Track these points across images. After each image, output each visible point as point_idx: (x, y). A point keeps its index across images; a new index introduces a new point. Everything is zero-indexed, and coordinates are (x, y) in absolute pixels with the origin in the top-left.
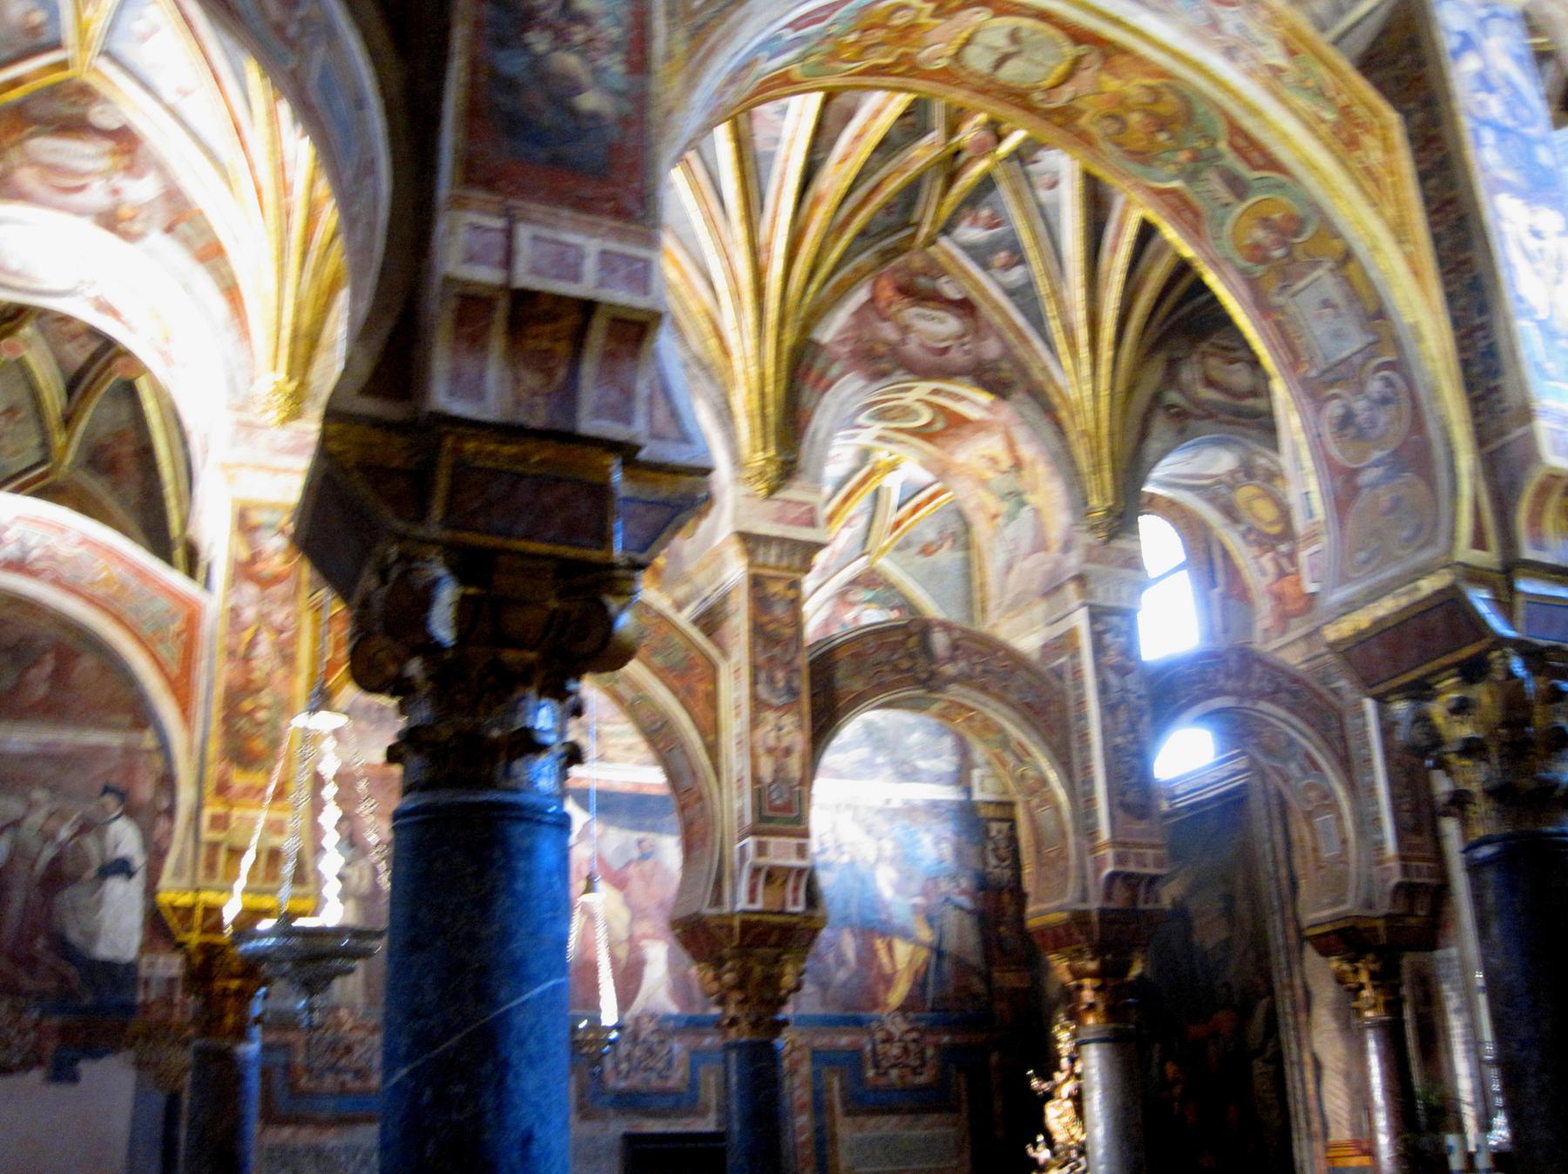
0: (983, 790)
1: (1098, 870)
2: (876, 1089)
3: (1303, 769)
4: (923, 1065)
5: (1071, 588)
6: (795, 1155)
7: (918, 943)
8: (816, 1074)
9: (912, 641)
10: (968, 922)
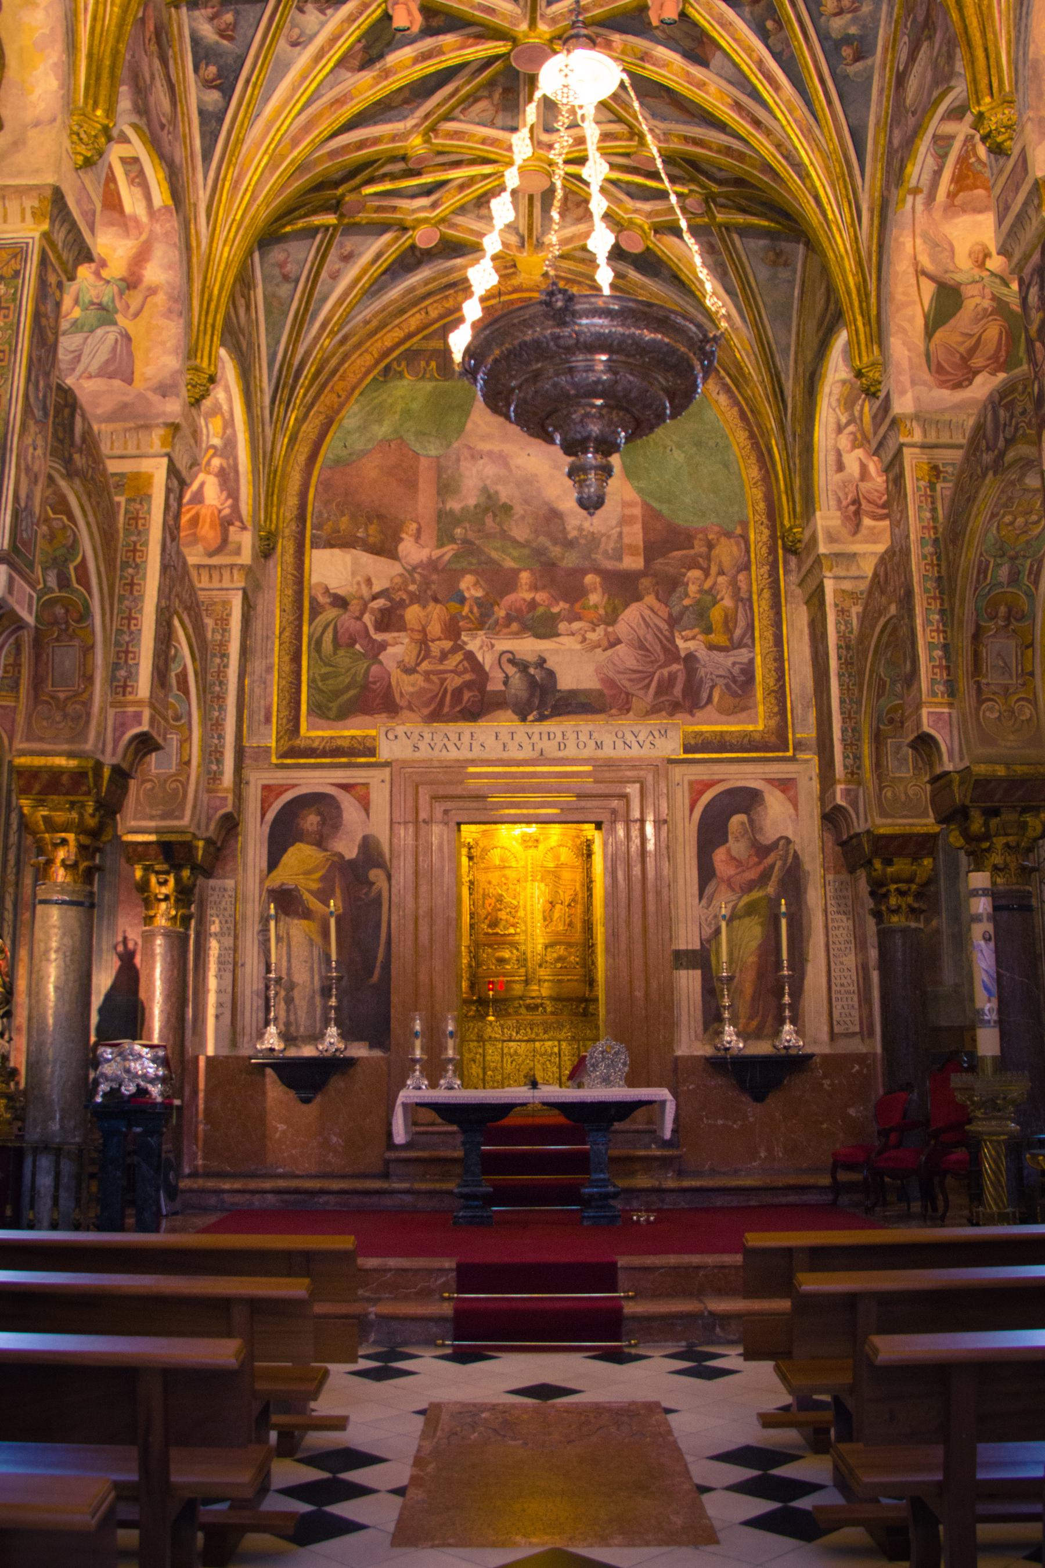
1: (121, 727)
9: (67, 411)
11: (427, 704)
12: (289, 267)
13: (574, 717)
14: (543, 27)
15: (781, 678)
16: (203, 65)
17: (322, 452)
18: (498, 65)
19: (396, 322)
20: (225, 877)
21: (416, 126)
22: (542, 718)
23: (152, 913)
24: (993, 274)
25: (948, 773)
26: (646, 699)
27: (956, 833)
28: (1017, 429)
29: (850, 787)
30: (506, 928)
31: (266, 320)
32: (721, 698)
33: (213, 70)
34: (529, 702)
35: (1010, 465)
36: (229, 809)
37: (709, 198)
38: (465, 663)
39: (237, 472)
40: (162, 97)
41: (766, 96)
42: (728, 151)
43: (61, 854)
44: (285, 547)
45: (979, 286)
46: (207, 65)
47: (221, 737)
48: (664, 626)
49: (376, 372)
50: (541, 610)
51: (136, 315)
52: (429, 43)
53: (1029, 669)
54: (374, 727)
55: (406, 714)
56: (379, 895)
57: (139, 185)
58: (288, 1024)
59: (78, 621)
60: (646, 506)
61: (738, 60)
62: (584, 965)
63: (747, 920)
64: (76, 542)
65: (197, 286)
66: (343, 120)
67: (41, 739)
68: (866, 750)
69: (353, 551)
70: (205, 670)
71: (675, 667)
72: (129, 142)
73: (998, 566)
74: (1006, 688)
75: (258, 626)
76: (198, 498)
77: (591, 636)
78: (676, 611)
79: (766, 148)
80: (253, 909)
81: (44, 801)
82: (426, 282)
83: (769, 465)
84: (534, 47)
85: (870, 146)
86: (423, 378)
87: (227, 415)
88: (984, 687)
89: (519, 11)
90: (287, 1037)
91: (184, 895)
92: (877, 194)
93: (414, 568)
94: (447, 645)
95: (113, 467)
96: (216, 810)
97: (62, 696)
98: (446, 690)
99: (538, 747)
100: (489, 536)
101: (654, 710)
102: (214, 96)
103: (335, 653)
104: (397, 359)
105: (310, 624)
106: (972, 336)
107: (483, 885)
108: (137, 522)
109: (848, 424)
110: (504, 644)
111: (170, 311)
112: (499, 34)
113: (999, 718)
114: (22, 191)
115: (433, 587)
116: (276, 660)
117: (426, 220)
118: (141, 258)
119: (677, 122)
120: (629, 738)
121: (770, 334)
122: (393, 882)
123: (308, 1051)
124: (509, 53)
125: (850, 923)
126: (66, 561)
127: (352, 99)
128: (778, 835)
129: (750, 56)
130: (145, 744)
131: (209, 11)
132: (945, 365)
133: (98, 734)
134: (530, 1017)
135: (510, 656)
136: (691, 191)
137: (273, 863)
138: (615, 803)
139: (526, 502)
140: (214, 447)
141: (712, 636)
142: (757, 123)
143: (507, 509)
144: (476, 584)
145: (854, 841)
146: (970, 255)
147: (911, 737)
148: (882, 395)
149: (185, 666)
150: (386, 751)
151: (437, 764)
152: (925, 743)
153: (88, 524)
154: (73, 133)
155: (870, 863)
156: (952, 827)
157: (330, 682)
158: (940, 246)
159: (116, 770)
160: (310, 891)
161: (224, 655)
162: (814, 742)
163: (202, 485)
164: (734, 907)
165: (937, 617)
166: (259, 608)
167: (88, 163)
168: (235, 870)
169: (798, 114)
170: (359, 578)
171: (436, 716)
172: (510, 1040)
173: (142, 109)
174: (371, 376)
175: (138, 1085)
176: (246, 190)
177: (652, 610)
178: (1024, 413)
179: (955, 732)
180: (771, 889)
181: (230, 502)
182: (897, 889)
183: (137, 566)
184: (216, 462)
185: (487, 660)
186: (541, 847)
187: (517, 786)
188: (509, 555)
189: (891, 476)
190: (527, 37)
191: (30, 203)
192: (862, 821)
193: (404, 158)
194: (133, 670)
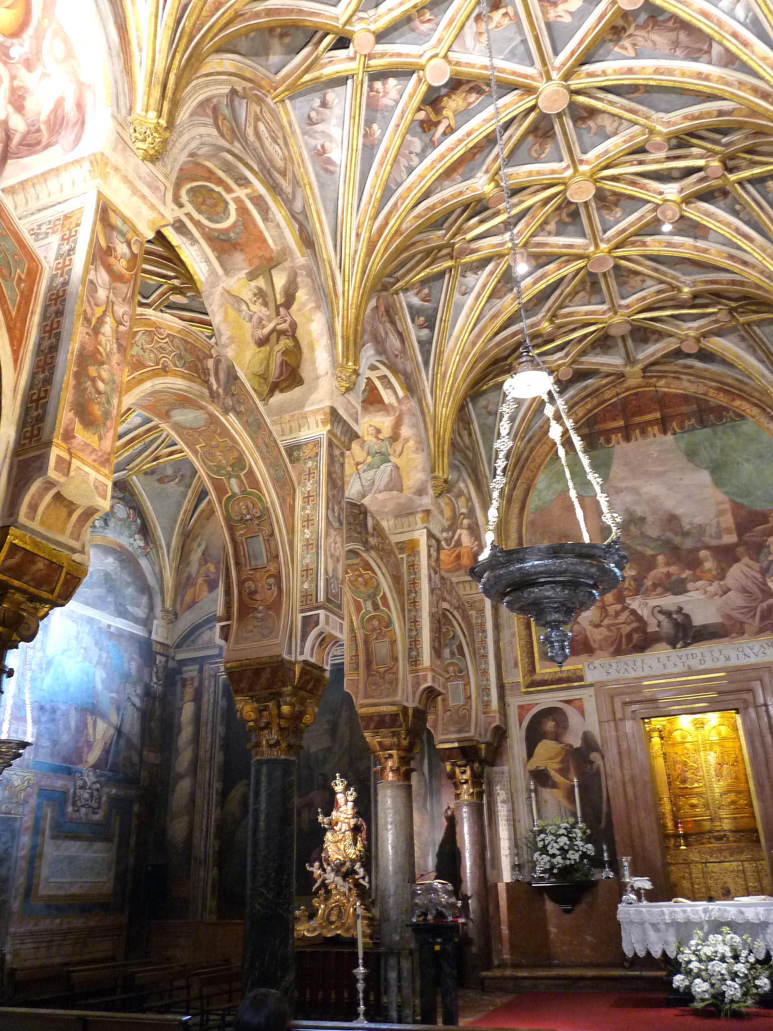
0: (157, 634)
1: (417, 684)
2: (71, 820)
3: (452, 654)
4: (99, 808)
5: (419, 517)
6: (15, 867)
7: (109, 723)
8: (39, 806)
9: (361, 516)
10: (136, 715)
11: (612, 644)
12: (490, 408)
13: (706, 642)
14: (603, 246)
16: (416, 318)
18: (583, 272)
22: (686, 645)
33: (422, 319)
34: (676, 636)
37: (731, 311)
38: (631, 617)
39: (477, 525)
40: (394, 340)
41: (745, 247)
42: (733, 282)
43: (390, 763)
47: (488, 680)
48: (759, 576)
51: (400, 455)
52: (540, 272)
55: (598, 652)
57: (389, 388)
59: (386, 627)
61: (722, 232)
64: (378, 584)
65: (431, 433)
66: (498, 326)
67: (372, 697)
70: (473, 641)
72: (378, 368)
76: (459, 543)
77: (709, 589)
78: (765, 564)
79: (753, 276)
80: (522, 781)
84: (600, 258)
89: (587, 241)
91: (477, 779)
95: (394, 539)
96: (490, 724)
97: (382, 670)
98: (621, 636)
100: (634, 537)
101: (761, 631)
102: (426, 332)
108: (413, 567)
110: (654, 602)
111: (417, 449)
112: (579, 257)
114: (315, 412)
117: (563, 364)
118: (397, 425)
119: (699, 274)
120: (748, 651)
126: (375, 595)
129: (729, 228)
130: (431, 694)
131: (415, 291)
133: (403, 690)
135: (659, 609)
137: (530, 754)
138: (746, 696)
139: (654, 513)
140: (463, 514)
142: (745, 263)
143: (642, 520)
149: (460, 642)
150: (589, 678)
153: (383, 574)
159: (416, 710)
160: (554, 770)
161: (484, 631)
163: (460, 535)
167: (348, 390)
168: (508, 760)
171: (618, 652)
173: (381, 350)
177: (748, 566)
181: (476, 543)
183: (416, 592)
184: (466, 522)
185: (644, 613)
186: (706, 726)
188: (648, 546)
191: (320, 417)
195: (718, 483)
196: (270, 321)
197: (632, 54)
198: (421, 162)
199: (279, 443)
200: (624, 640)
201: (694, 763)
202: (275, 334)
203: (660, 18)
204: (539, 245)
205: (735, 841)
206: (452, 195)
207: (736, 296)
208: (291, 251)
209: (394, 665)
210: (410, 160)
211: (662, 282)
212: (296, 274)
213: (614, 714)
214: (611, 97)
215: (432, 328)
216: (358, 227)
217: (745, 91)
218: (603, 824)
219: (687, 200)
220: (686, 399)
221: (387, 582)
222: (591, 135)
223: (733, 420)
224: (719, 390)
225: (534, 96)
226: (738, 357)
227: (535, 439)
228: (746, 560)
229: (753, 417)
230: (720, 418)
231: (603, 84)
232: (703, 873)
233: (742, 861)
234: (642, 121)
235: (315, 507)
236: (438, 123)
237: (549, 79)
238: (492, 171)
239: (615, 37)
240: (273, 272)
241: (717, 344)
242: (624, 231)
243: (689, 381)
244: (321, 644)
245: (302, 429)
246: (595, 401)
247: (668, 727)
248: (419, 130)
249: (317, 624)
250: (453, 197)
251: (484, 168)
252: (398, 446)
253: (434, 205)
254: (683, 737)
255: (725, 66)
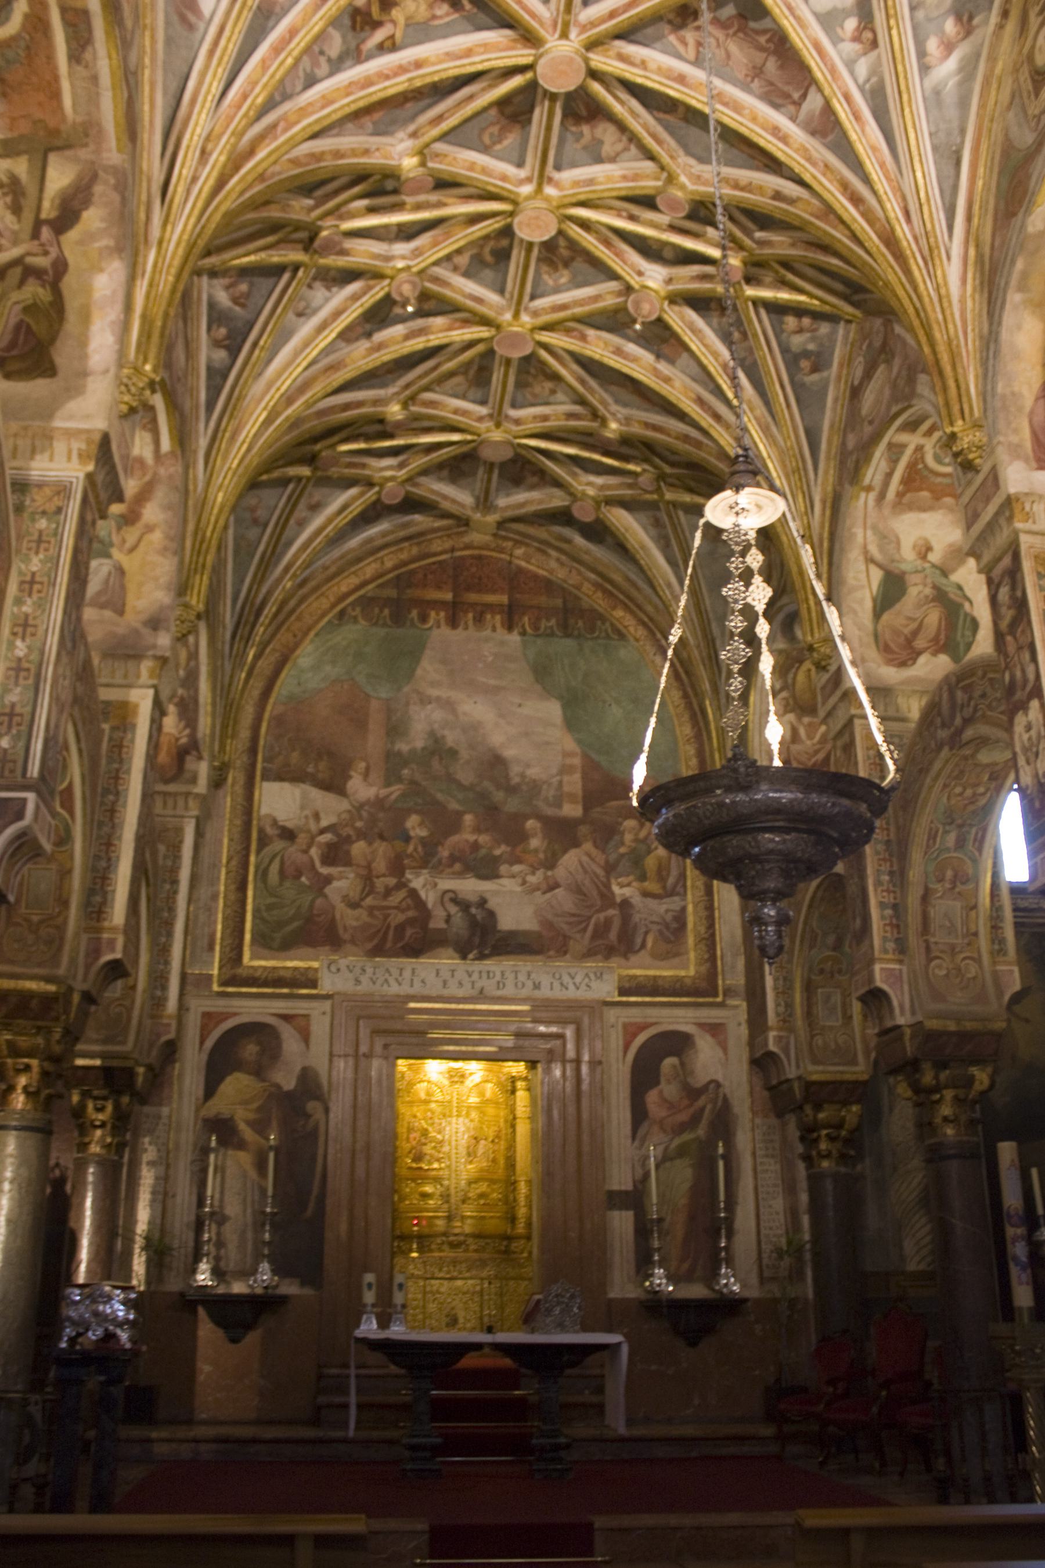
1: (95, 951)
5: (146, 666)
13: (512, 957)
14: (525, 318)
15: (711, 926)
16: (214, 327)
17: (276, 689)
19: (353, 569)
20: (161, 1105)
21: (397, 394)
22: (482, 957)
23: (87, 1140)
24: (934, 566)
25: (898, 1027)
26: (581, 942)
27: (904, 1084)
28: (975, 710)
29: (782, 1034)
30: (430, 1163)
31: (235, 561)
32: (655, 942)
33: (223, 331)
35: (967, 743)
36: (172, 1035)
37: (661, 477)
38: (409, 901)
42: (686, 439)
43: (22, 1081)
44: (235, 778)
45: (921, 575)
46: (219, 326)
47: (167, 963)
48: (600, 872)
49: (331, 615)
50: (483, 852)
52: (420, 322)
53: (973, 929)
54: (316, 960)
55: (349, 947)
56: (316, 1128)
58: (217, 1259)
60: (585, 756)
62: (506, 1202)
63: (678, 1162)
65: (191, 527)
66: (335, 384)
67: (12, 962)
68: (798, 997)
69: (303, 786)
71: (611, 912)
73: (946, 832)
74: (953, 948)
75: (205, 853)
77: (532, 879)
78: (613, 857)
80: (187, 1137)
81: (10, 1025)
82: (384, 534)
83: (702, 724)
84: (517, 334)
85: (824, 446)
86: (376, 624)
87: (192, 648)
88: (933, 946)
90: (217, 1272)
91: (121, 1122)
92: (830, 488)
93: (362, 806)
94: (392, 881)
95: (105, 694)
96: (159, 1035)
97: (35, 919)
98: (389, 927)
99: (478, 985)
101: (590, 954)
102: (221, 355)
103: (281, 885)
104: (353, 605)
105: (258, 852)
106: (914, 620)
107: (407, 1118)
108: (119, 750)
109: (781, 690)
110: (446, 884)
112: (485, 321)
113: (947, 975)
114: (70, 434)
115: (381, 824)
116: (222, 888)
119: (638, 408)
120: (566, 979)
121: (708, 602)
122: (332, 1115)
123: (238, 1288)
124: (492, 338)
125: (778, 1167)
127: (345, 366)
128: (708, 1079)
129: (716, 359)
130: (117, 970)
132: (892, 645)
134: (448, 1253)
135: (451, 895)
136: (644, 470)
137: (210, 1091)
141: (646, 884)
143: (453, 753)
144: (421, 824)
145: (784, 1087)
146: (914, 547)
147: (862, 991)
148: (833, 668)
150: (327, 984)
151: (377, 998)
152: (875, 999)
153: (80, 751)
154: (122, 383)
155: (801, 1108)
156: (900, 1078)
157: (275, 912)
158: (888, 539)
161: (175, 882)
162: (742, 989)
164: (666, 1149)
165: (887, 878)
166: (208, 836)
169: (758, 412)
170: (307, 812)
171: (378, 951)
172: (433, 1278)
174: (326, 619)
175: (106, 1330)
176: (244, 442)
177: (589, 855)
178: (983, 696)
179: (906, 987)
180: (701, 1132)
181: (187, 731)
182: (827, 1135)
185: (430, 898)
186: (470, 1082)
187: (453, 1021)
189: (840, 743)
190: (510, 325)
191: (77, 445)
192: (793, 1068)
193: (381, 421)
194: (109, 897)
195: (571, 723)
196: (15, 243)
197: (691, 54)
198: (331, 74)
199: (8, 472)
200: (391, 933)
201: (439, 1132)
202: (18, 271)
203: (752, 25)
204: (436, 280)
205: (476, 1251)
206: (353, 150)
207: (676, 458)
208: (100, 131)
209: (60, 913)
210: (315, 64)
211: (582, 402)
212: (94, 177)
213: (357, 1045)
214: (634, 104)
215: (234, 352)
216: (208, 139)
217: (830, 181)
218: (309, 1212)
219: (674, 299)
220: (548, 586)
221: (82, 765)
222: (578, 146)
223: (608, 637)
224: (597, 586)
225: (533, 52)
226: (643, 547)
227: (312, 584)
228: (588, 846)
229: (637, 640)
230: (592, 629)
231: (639, 80)
232: (425, 1293)
233: (482, 1279)
234: (666, 159)
235: (43, 605)
236: (377, 25)
237: (564, 35)
238: (426, 138)
239: (678, 20)
240: (53, 158)
241: (623, 520)
242: (564, 307)
243: (558, 560)
244: (13, 855)
245: (38, 457)
246: (415, 551)
247: (409, 1075)
248: (347, 22)
249: (20, 816)
250: (354, 153)
251: (412, 128)
252: (131, 535)
253: (323, 153)
254: (429, 1094)
255: (813, 133)
